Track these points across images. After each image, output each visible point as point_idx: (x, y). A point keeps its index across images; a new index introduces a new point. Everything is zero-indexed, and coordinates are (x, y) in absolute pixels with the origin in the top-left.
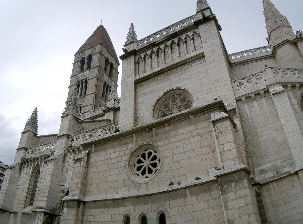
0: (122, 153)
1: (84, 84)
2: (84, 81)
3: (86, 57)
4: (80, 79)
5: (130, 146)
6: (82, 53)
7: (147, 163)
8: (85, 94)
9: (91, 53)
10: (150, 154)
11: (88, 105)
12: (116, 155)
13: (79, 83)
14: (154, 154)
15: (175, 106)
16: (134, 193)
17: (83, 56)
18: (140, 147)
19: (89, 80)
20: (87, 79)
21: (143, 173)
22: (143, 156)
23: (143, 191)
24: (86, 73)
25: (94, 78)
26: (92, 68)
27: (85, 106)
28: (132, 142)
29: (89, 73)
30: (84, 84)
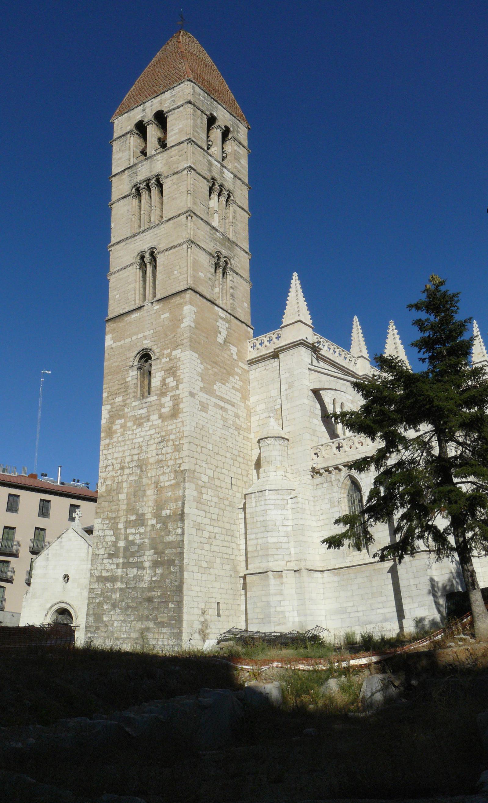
9: (231, 129)
11: (242, 277)
17: (215, 114)
27: (237, 273)
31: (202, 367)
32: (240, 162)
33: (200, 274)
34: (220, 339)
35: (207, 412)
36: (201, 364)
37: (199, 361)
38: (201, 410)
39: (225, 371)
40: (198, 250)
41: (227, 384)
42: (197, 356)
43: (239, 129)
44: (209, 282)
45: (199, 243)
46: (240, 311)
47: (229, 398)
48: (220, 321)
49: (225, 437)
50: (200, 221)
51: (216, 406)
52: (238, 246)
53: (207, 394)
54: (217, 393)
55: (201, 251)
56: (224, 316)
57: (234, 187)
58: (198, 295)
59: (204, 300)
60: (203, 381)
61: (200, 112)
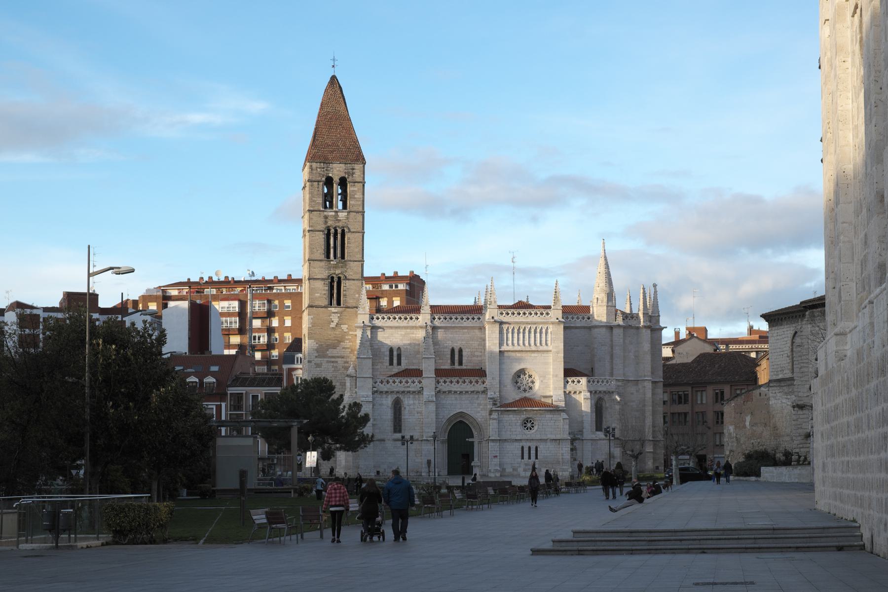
0: (518, 419)
1: (339, 236)
2: (339, 231)
3: (336, 179)
4: (330, 223)
5: (522, 416)
6: (325, 164)
7: (529, 425)
8: (343, 257)
9: (346, 176)
10: (531, 421)
11: (354, 280)
12: (515, 419)
13: (329, 230)
14: (532, 422)
15: (524, 379)
16: (525, 437)
17: (330, 175)
18: (527, 418)
19: (350, 231)
20: (346, 230)
21: (527, 429)
22: (527, 421)
23: (528, 437)
24: (342, 215)
25: (358, 232)
26: (353, 212)
27: (349, 280)
28: (523, 414)
29: (348, 218)
30: (339, 236)
31: (317, 345)
32: (356, 198)
33: (316, 295)
34: (333, 325)
35: (321, 367)
36: (317, 344)
37: (315, 343)
38: (316, 367)
39: (336, 341)
40: (315, 281)
41: (338, 348)
42: (313, 341)
43: (354, 171)
44: (324, 296)
45: (315, 277)
46: (351, 301)
47: (340, 355)
48: (333, 315)
49: (335, 376)
50: (316, 262)
51: (328, 362)
52: (350, 261)
53: (321, 358)
54: (329, 355)
55: (317, 281)
56: (336, 311)
57: (348, 221)
58: (314, 308)
59: (320, 308)
60: (317, 352)
61: (317, 183)
